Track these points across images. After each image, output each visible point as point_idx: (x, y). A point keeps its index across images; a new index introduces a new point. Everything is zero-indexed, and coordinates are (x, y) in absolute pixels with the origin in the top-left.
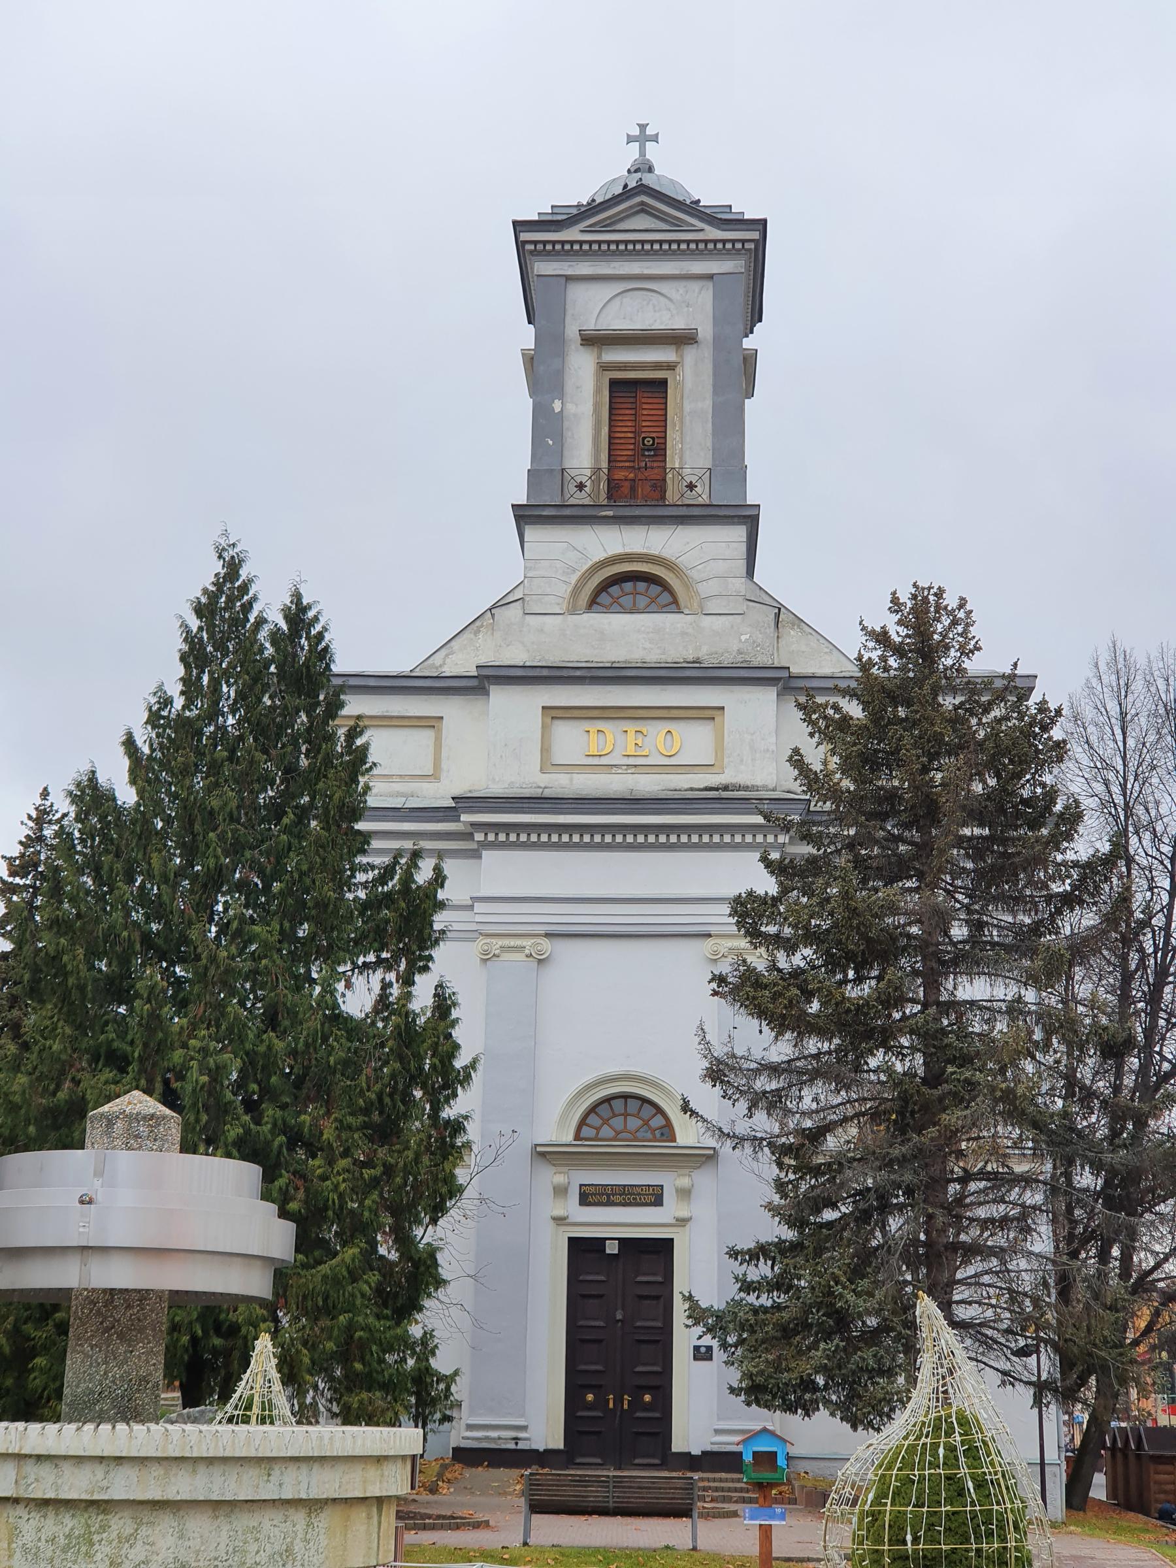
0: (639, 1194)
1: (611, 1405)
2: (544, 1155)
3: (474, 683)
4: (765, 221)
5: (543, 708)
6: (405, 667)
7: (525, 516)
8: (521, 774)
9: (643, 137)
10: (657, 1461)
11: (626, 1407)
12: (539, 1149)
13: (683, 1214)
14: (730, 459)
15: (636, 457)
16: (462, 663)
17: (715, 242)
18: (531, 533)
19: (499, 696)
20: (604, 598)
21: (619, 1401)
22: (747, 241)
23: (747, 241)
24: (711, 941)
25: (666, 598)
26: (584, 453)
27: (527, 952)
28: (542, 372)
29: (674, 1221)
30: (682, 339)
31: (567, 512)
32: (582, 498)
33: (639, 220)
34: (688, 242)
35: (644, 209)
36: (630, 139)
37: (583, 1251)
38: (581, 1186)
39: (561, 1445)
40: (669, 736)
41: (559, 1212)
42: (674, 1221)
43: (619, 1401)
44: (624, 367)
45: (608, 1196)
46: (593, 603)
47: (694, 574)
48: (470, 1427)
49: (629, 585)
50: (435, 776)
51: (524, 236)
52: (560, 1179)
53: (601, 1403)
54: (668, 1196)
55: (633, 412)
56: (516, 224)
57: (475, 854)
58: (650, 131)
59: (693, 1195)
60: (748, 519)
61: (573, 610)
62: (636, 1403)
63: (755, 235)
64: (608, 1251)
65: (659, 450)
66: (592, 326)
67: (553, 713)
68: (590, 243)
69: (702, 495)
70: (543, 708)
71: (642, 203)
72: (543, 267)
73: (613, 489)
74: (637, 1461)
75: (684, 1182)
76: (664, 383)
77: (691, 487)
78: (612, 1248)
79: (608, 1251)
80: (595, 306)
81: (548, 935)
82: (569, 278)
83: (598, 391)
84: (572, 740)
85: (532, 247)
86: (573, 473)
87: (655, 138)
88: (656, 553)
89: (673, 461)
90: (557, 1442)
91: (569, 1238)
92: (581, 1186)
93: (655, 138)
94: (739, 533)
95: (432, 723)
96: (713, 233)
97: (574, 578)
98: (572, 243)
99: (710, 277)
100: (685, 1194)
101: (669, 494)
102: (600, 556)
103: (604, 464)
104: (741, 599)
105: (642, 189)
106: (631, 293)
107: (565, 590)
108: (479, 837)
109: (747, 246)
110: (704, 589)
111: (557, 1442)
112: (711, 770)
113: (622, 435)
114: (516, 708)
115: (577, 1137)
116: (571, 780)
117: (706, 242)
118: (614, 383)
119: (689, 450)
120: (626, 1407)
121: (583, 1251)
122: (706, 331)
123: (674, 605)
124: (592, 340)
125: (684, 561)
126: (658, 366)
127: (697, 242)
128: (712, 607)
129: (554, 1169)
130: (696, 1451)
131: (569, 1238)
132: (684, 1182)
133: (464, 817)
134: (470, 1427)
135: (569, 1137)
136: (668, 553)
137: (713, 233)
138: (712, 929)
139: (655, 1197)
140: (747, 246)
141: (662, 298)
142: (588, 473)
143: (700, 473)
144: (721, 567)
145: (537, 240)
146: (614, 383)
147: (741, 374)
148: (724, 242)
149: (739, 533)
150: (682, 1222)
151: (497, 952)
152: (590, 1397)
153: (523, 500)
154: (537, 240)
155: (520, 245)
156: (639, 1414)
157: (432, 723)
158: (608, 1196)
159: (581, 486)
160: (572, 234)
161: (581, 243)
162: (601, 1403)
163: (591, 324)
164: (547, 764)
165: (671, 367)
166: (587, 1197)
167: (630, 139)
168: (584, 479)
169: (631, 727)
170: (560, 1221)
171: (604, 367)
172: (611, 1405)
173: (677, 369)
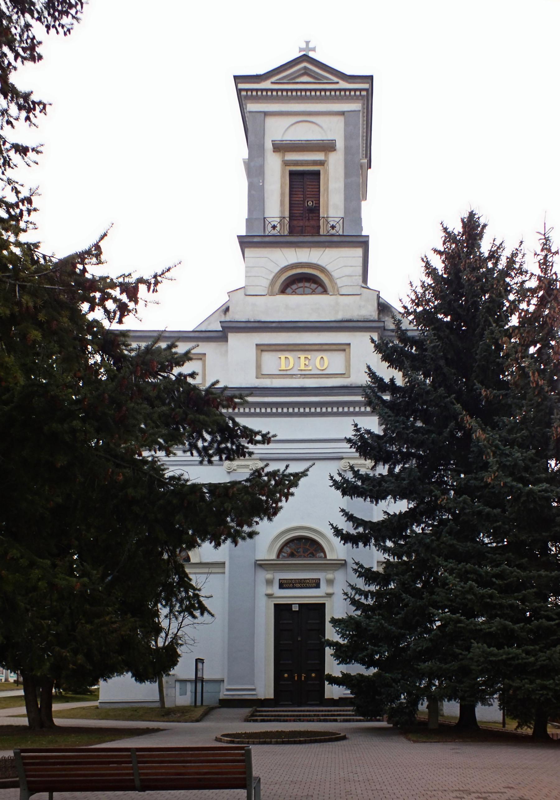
0: (308, 583)
1: (296, 678)
2: (261, 565)
3: (220, 334)
4: (372, 77)
6: (190, 327)
7: (245, 242)
10: (318, 702)
11: (303, 679)
12: (258, 562)
13: (330, 591)
14: (353, 213)
15: (304, 211)
17: (345, 90)
18: (247, 251)
21: (300, 677)
22: (362, 89)
23: (362, 89)
24: (343, 461)
25: (320, 289)
26: (275, 208)
28: (254, 170)
29: (325, 595)
31: (267, 239)
33: (304, 79)
35: (306, 72)
37: (281, 610)
38: (280, 580)
39: (272, 697)
40: (322, 360)
41: (269, 591)
42: (325, 595)
43: (300, 677)
44: (296, 163)
45: (293, 584)
46: (283, 291)
47: (335, 274)
48: (228, 690)
49: (302, 280)
51: (241, 86)
52: (269, 576)
53: (291, 677)
54: (323, 584)
55: (302, 186)
56: (236, 77)
59: (335, 584)
60: (363, 243)
61: (271, 294)
62: (308, 677)
63: (366, 86)
64: (293, 609)
65: (315, 211)
66: (280, 138)
67: (262, 348)
68: (277, 90)
70: (257, 345)
71: (305, 68)
72: (252, 107)
73: (292, 231)
74: (309, 703)
75: (330, 576)
77: (333, 227)
78: (295, 608)
79: (293, 609)
83: (283, 176)
84: (273, 363)
86: (269, 220)
88: (315, 262)
90: (271, 696)
91: (276, 605)
92: (280, 580)
94: (359, 252)
96: (343, 85)
97: (271, 277)
99: (342, 113)
100: (330, 582)
101: (321, 230)
102: (284, 264)
103: (287, 214)
104: (359, 287)
105: (305, 58)
106: (300, 124)
107: (266, 283)
110: (339, 283)
111: (271, 696)
112: (343, 376)
113: (297, 202)
114: (242, 346)
115: (278, 556)
116: (272, 383)
117: (340, 90)
120: (303, 679)
121: (281, 610)
123: (325, 291)
125: (329, 268)
127: (335, 90)
129: (266, 572)
130: (336, 698)
131: (276, 605)
132: (330, 576)
134: (228, 690)
135: (274, 556)
136: (321, 263)
137: (343, 85)
138: (344, 455)
139: (316, 584)
141: (317, 127)
142: (278, 220)
143: (337, 220)
144: (348, 271)
145: (249, 89)
148: (350, 90)
149: (359, 252)
150: (329, 595)
152: (286, 675)
153: (244, 233)
154: (249, 89)
155: (239, 91)
156: (309, 682)
158: (293, 584)
159: (274, 227)
160: (266, 85)
162: (291, 677)
163: (278, 137)
164: (260, 375)
166: (283, 585)
168: (276, 223)
169: (302, 356)
170: (269, 596)
171: (286, 163)
172: (296, 678)
173: (326, 165)
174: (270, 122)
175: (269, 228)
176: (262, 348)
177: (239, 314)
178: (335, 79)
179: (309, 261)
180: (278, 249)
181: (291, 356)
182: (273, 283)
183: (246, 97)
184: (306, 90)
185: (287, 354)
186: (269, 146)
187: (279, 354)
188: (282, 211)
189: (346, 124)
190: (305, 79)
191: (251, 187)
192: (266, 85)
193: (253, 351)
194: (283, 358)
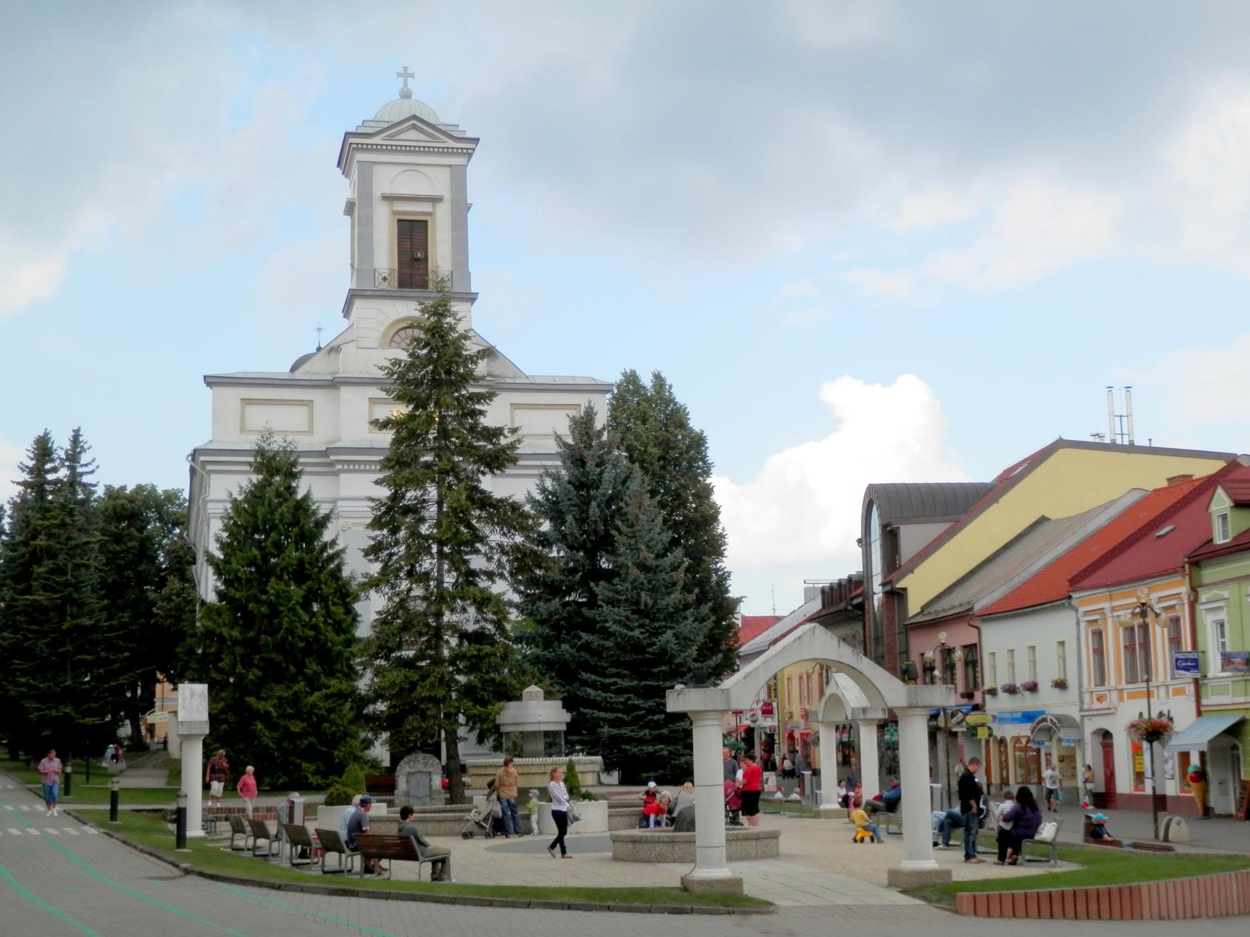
9: (406, 74)
16: (319, 369)
19: (345, 392)
26: (385, 258)
30: (435, 200)
32: (385, 286)
35: (414, 127)
36: (399, 75)
50: (310, 431)
57: (336, 474)
58: (409, 71)
76: (426, 222)
80: (392, 178)
87: (412, 76)
93: (412, 76)
95: (308, 403)
97: (382, 329)
102: (395, 317)
103: (396, 267)
107: (377, 335)
118: (399, 221)
119: (440, 257)
122: (447, 196)
124: (386, 198)
126: (423, 214)
146: (399, 221)
147: (461, 209)
157: (308, 403)
159: (385, 279)
163: (388, 191)
165: (430, 214)
167: (399, 75)
182: (384, 335)
190: (413, 135)
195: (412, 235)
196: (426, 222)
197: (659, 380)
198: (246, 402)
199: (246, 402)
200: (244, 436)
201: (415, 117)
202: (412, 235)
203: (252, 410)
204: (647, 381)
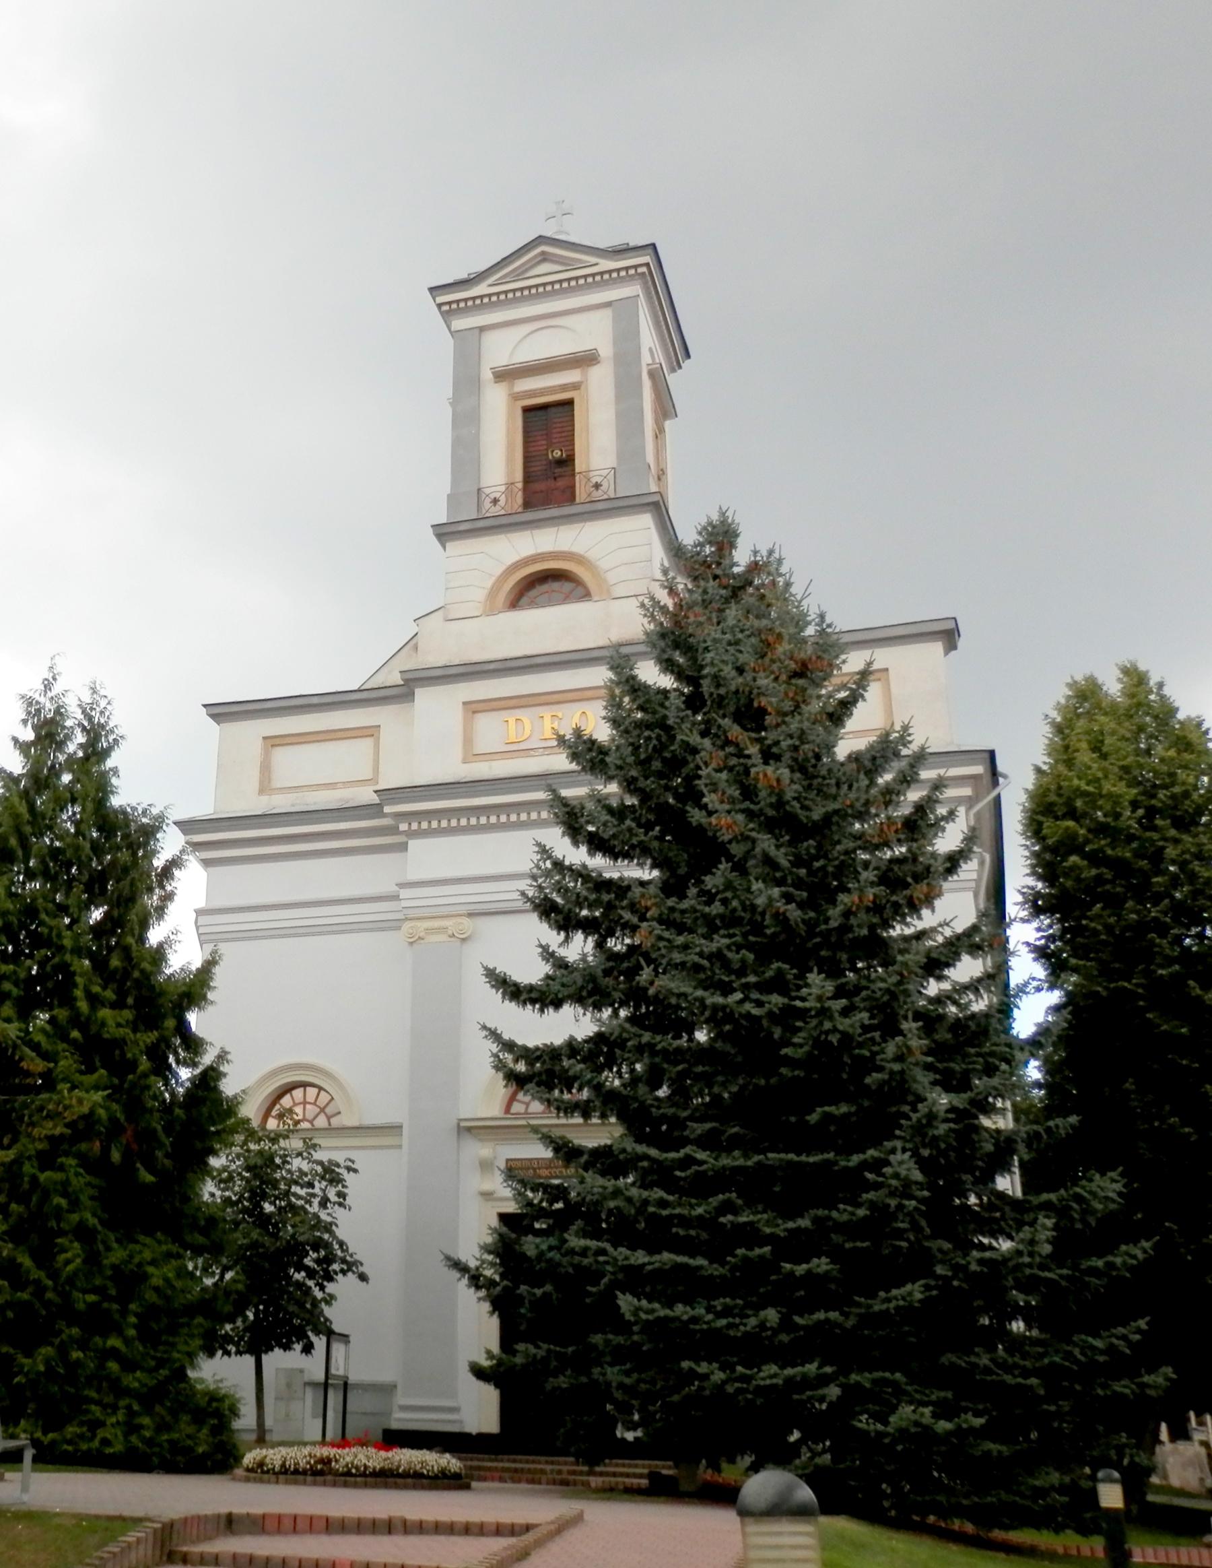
5: (464, 703)
8: (447, 765)
17: (610, 272)
20: (524, 600)
27: (450, 932)
30: (587, 360)
32: (496, 510)
34: (585, 277)
35: (545, 258)
38: (508, 1160)
40: (584, 717)
41: (487, 1186)
45: (534, 1169)
47: (603, 564)
49: (544, 582)
51: (440, 300)
61: (490, 609)
67: (473, 708)
68: (498, 294)
69: (608, 490)
71: (543, 253)
72: (459, 323)
77: (597, 486)
81: (471, 915)
82: (482, 329)
84: (493, 731)
85: (446, 308)
86: (487, 491)
89: (579, 465)
92: (508, 1160)
95: (370, 732)
96: (607, 264)
97: (489, 583)
98: (481, 297)
102: (515, 558)
107: (480, 595)
108: (403, 827)
109: (640, 270)
110: (611, 578)
114: (438, 708)
117: (602, 273)
118: (527, 410)
122: (606, 351)
123: (586, 595)
124: (504, 375)
125: (592, 555)
126: (564, 388)
127: (593, 275)
128: (619, 591)
133: (387, 809)
136: (576, 549)
137: (607, 264)
140: (640, 270)
142: (503, 488)
146: (527, 410)
151: (422, 934)
157: (370, 732)
158: (534, 1169)
159: (495, 501)
161: (490, 295)
164: (470, 756)
165: (576, 386)
168: (497, 495)
170: (487, 1196)
171: (515, 397)
174: (490, 338)
175: (487, 504)
176: (473, 708)
177: (434, 655)
178: (593, 260)
179: (556, 549)
180: (502, 536)
181: (526, 715)
182: (492, 594)
183: (450, 312)
184: (544, 285)
185: (519, 713)
186: (487, 375)
187: (504, 715)
188: (510, 472)
189: (616, 320)
191: (457, 443)
192: (481, 289)
193: (458, 713)
194: (512, 721)
195: (548, 429)
196: (569, 403)
197: (1136, 679)
198: (273, 742)
199: (273, 742)
200: (264, 799)
201: (541, 240)
202: (548, 429)
203: (283, 757)
204: (1113, 686)
